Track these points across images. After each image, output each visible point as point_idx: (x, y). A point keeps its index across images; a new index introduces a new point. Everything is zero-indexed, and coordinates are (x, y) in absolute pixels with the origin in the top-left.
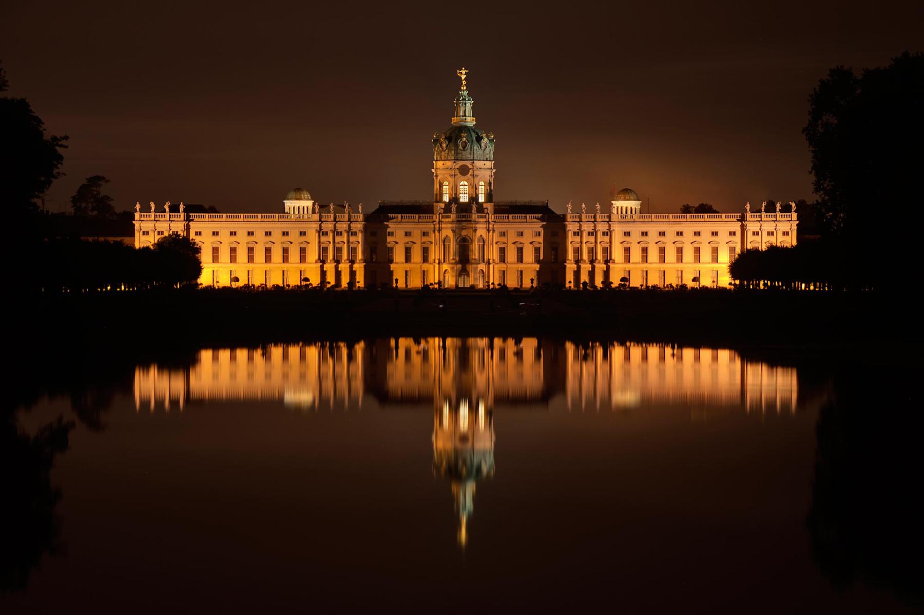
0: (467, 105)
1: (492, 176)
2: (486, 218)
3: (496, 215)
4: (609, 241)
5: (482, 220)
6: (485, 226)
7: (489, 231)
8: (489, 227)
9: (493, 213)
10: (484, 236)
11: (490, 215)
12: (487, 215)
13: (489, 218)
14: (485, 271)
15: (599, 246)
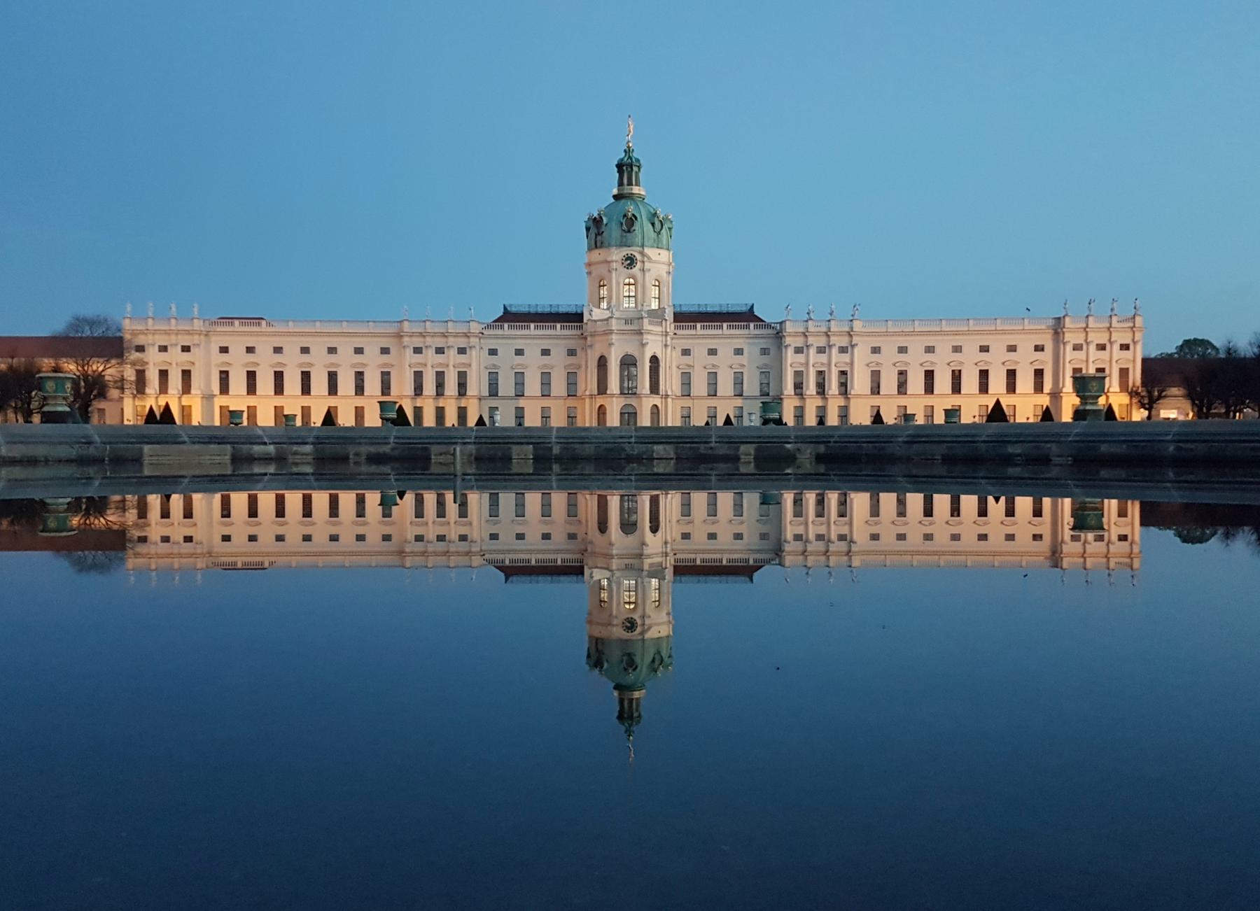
0: (634, 168)
1: (669, 273)
2: (662, 326)
3: (676, 324)
4: (848, 361)
5: (658, 329)
6: (660, 338)
7: (666, 346)
8: (666, 341)
9: (672, 321)
10: (659, 356)
11: (668, 323)
12: (664, 322)
13: (666, 328)
14: (659, 406)
15: (833, 368)
